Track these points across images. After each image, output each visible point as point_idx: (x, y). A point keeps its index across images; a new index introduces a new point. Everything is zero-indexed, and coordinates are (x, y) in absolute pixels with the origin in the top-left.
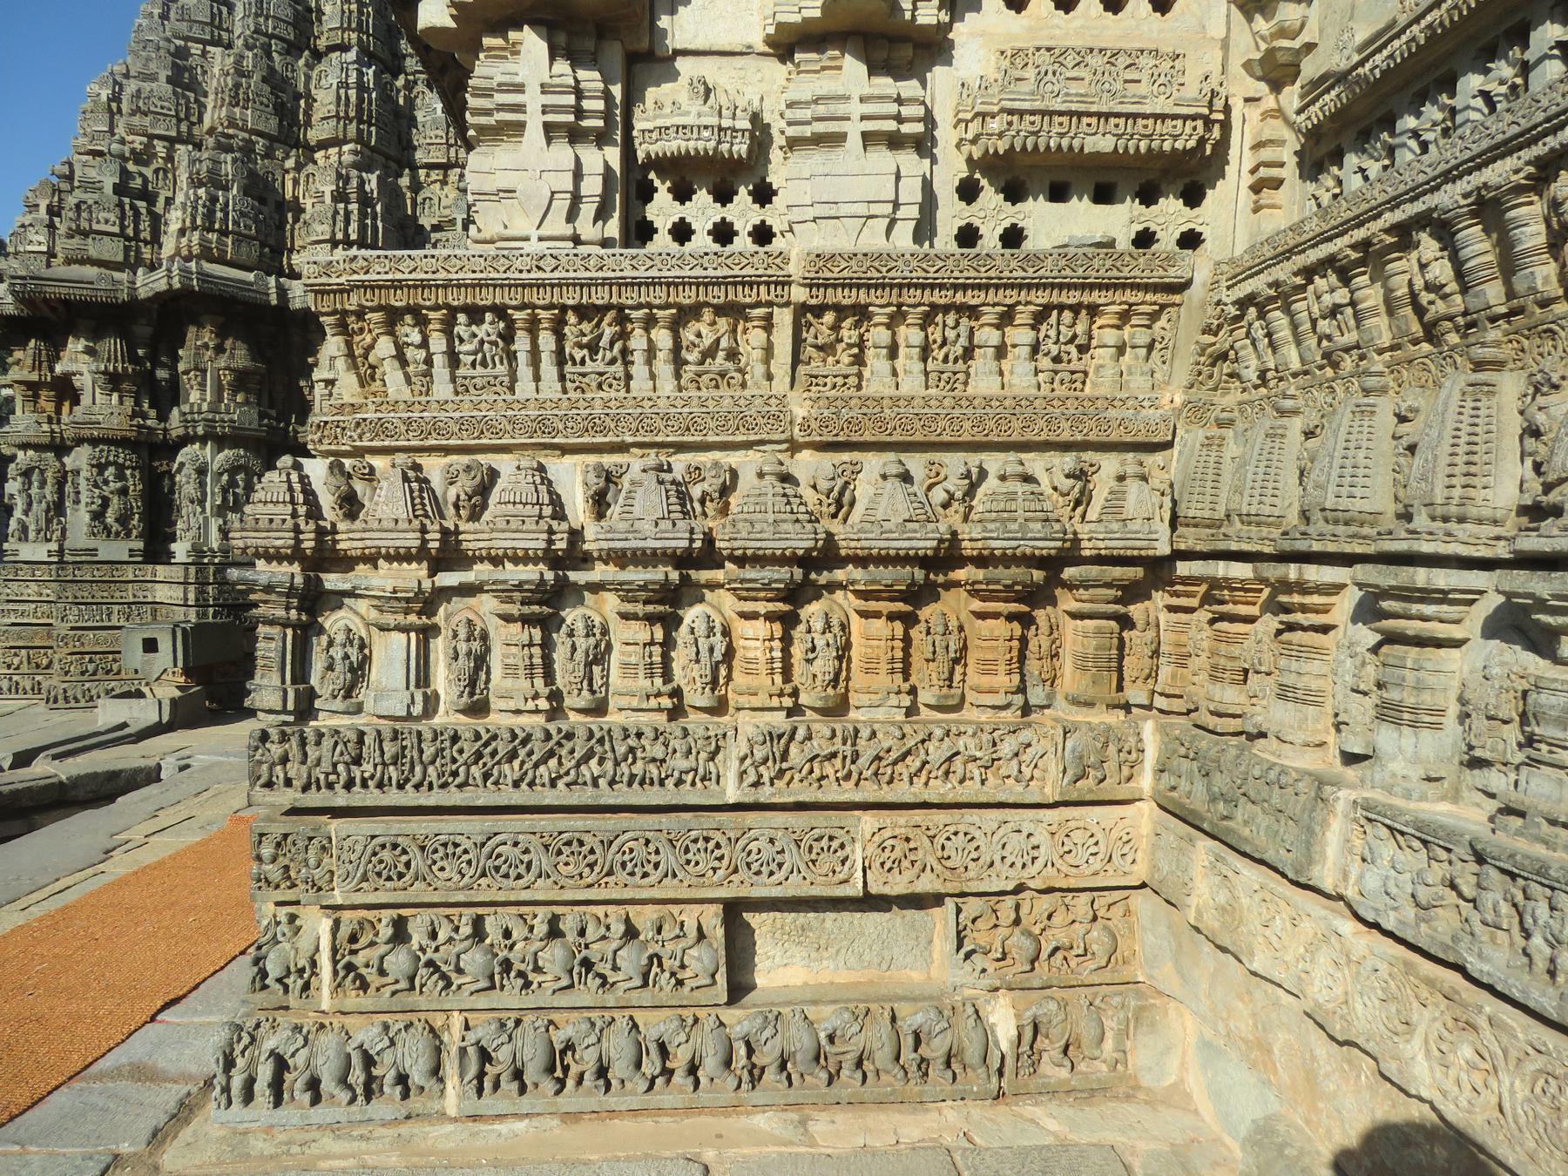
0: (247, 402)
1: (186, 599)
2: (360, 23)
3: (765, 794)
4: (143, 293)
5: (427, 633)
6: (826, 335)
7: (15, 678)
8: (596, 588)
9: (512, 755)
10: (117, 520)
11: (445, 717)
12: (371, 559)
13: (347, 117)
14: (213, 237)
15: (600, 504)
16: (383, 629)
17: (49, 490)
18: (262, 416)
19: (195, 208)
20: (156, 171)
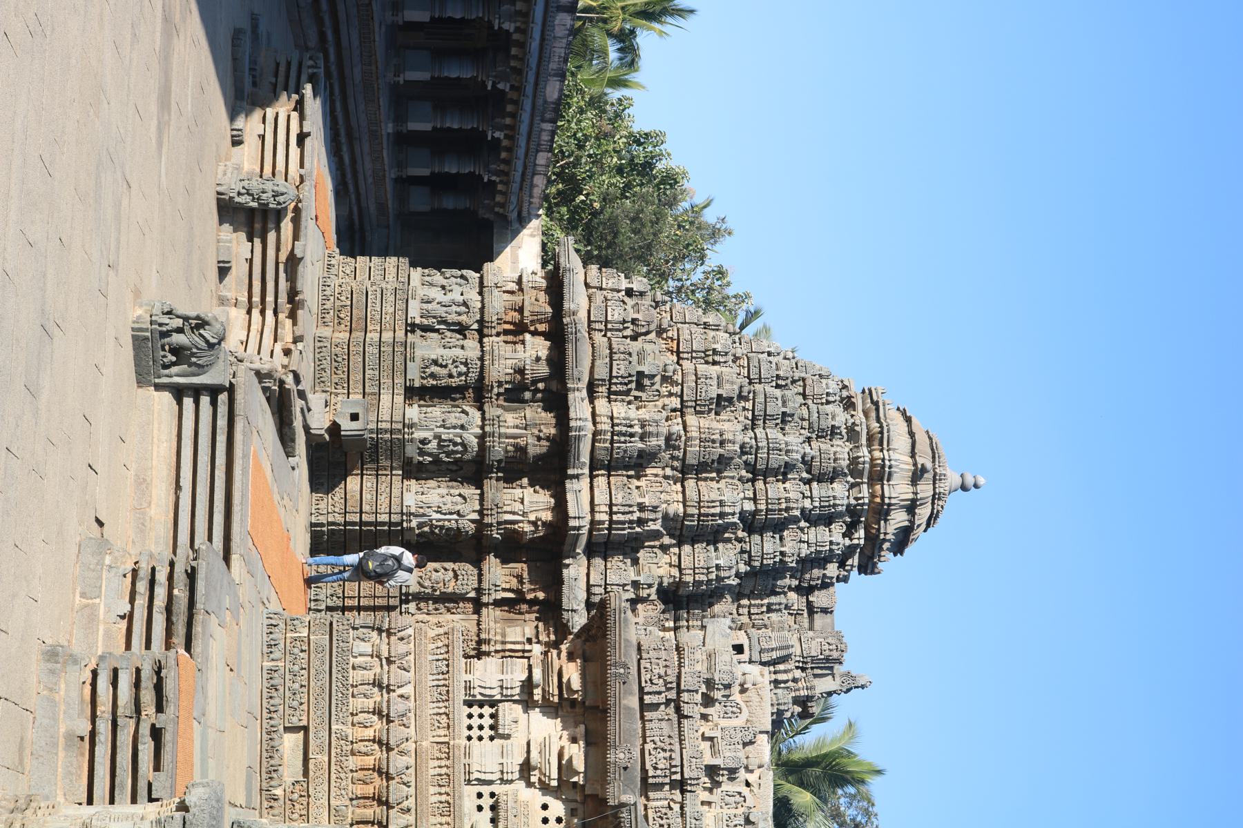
0: (507, 451)
1: (381, 422)
2: (772, 510)
3: (333, 735)
4: (571, 396)
5: (372, 656)
6: (443, 750)
7: (332, 298)
8: (382, 695)
9: (343, 677)
10: (433, 373)
11: (352, 660)
12: (388, 644)
13: (700, 508)
14: (608, 436)
15: (401, 696)
16: (373, 645)
17: (452, 318)
18: (499, 461)
19: (626, 425)
20: (658, 391)
